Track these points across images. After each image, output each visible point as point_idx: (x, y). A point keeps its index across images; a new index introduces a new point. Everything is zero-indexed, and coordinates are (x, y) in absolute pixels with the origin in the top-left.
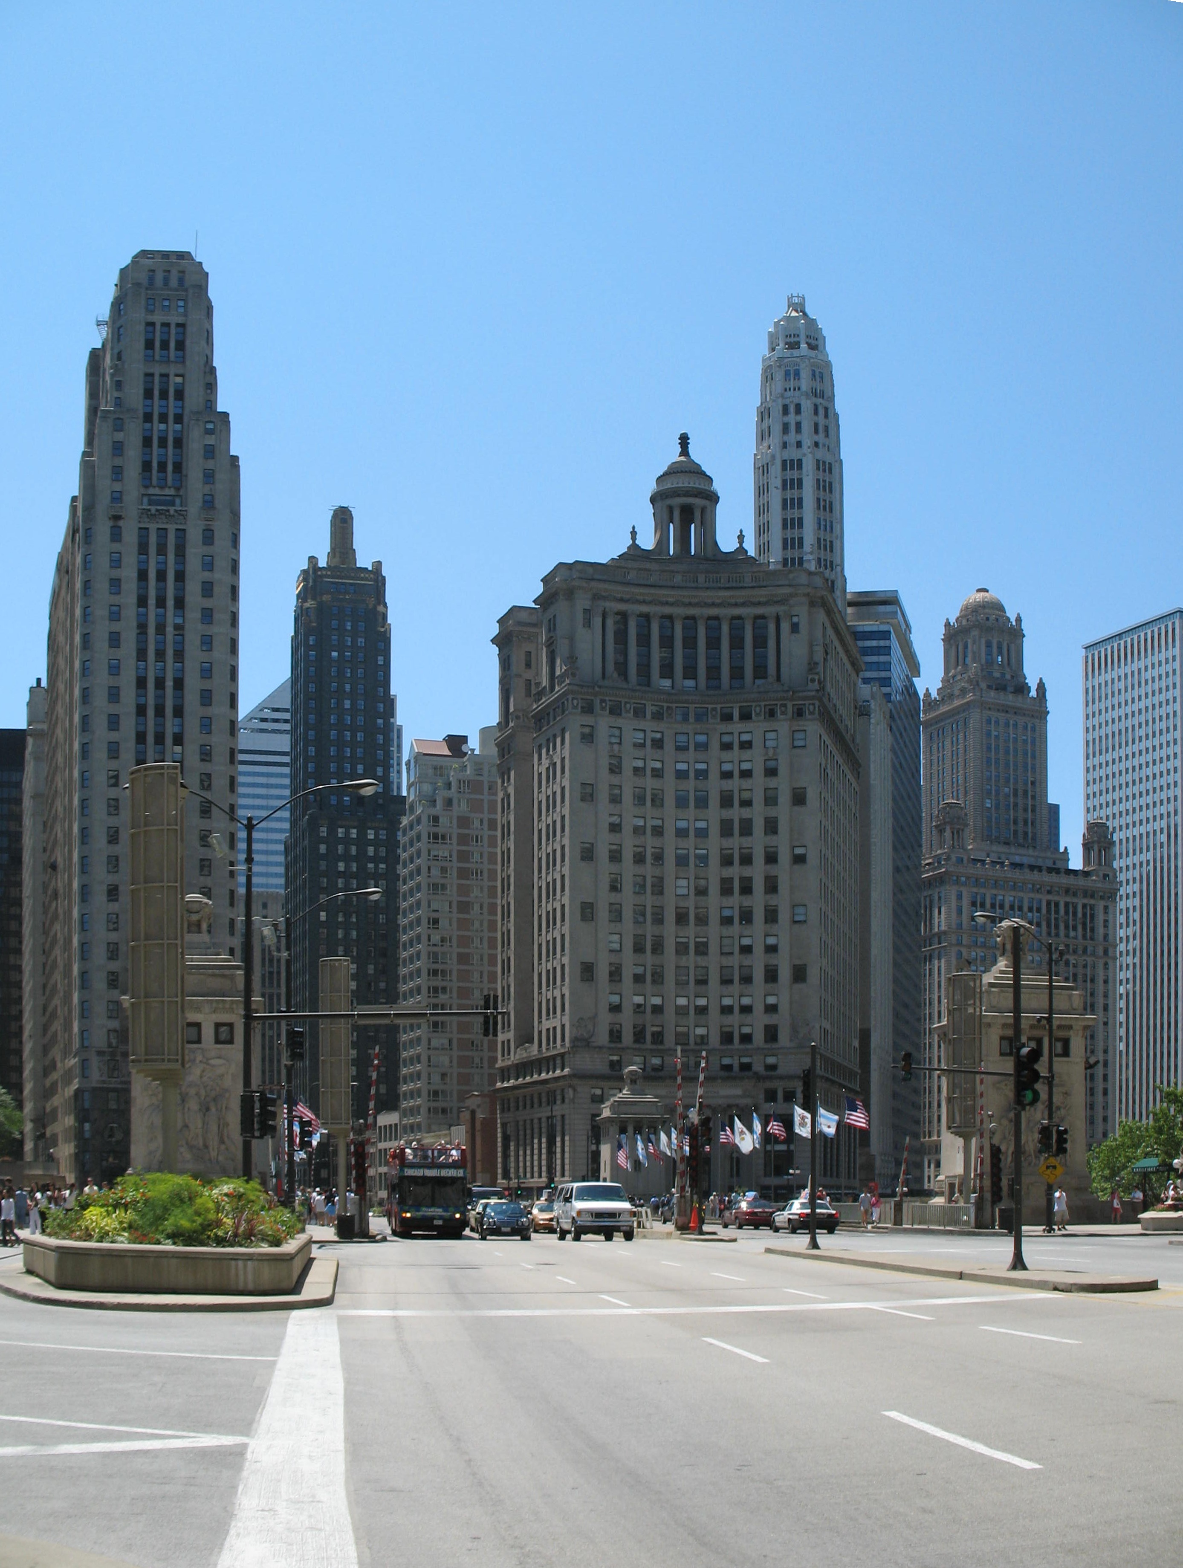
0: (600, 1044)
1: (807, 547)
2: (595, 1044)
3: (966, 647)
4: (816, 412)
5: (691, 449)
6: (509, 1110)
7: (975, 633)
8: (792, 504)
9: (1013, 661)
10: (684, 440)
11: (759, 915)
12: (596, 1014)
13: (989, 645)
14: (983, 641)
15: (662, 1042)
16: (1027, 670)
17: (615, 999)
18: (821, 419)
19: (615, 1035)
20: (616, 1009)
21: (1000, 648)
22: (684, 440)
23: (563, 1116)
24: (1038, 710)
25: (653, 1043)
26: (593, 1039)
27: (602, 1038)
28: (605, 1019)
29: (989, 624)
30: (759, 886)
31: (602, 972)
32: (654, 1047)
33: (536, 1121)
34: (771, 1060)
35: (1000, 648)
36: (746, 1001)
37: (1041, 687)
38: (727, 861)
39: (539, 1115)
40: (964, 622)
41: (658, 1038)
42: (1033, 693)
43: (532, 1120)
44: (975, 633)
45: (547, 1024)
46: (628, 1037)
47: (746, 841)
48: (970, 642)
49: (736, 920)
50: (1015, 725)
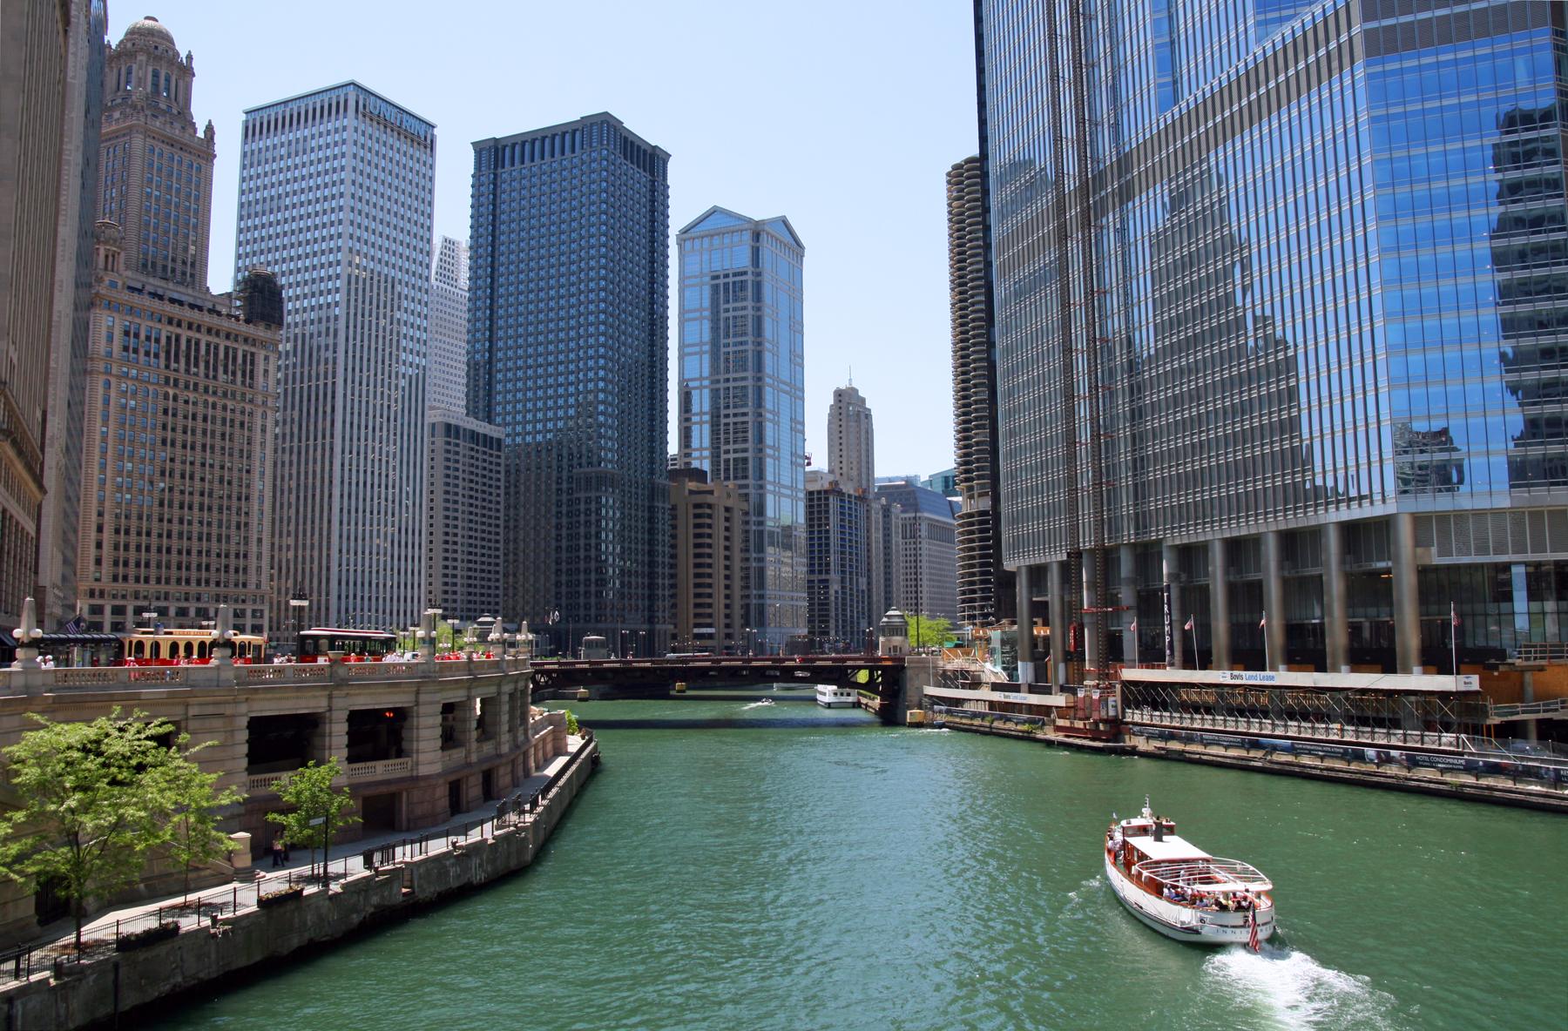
3: (129, 72)
7: (142, 58)
9: (180, 98)
13: (156, 75)
14: (150, 69)
16: (194, 109)
21: (168, 80)
24: (205, 151)
29: (158, 52)
35: (168, 80)
37: (210, 129)
40: (129, 45)
42: (200, 134)
44: (142, 58)
48: (135, 67)
50: (180, 162)
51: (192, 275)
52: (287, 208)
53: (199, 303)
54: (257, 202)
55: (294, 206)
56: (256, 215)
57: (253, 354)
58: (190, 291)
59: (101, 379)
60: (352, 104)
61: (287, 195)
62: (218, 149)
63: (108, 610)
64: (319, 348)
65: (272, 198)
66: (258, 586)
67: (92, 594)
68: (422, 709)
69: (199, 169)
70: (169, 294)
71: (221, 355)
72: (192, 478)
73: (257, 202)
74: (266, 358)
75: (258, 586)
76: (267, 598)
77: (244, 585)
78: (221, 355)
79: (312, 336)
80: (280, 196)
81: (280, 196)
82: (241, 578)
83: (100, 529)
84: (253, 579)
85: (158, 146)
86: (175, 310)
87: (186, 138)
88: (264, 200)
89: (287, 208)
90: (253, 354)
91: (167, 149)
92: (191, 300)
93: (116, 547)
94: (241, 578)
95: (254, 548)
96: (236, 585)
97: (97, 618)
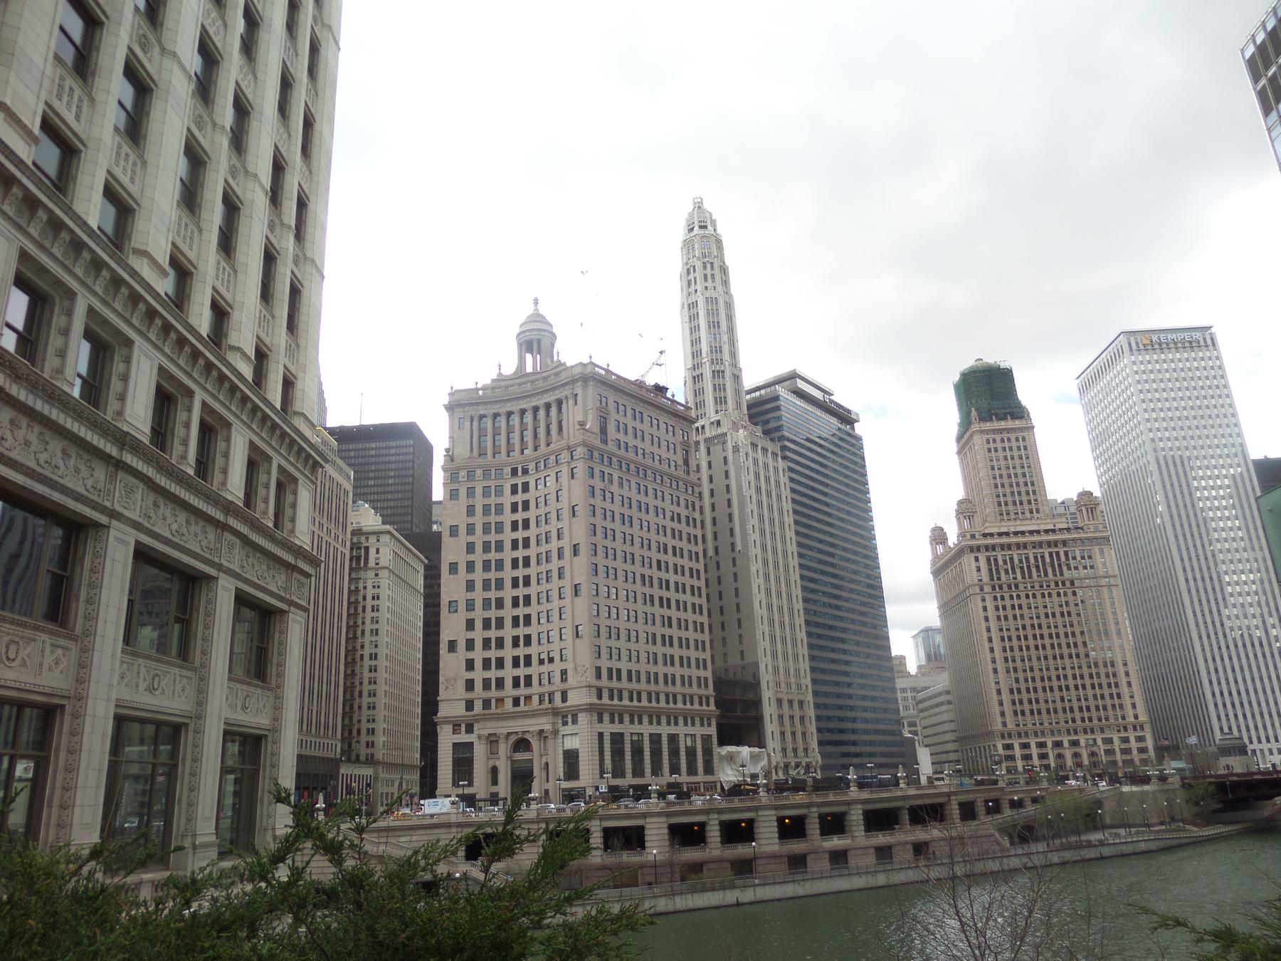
1: (704, 355)
4: (705, 268)
5: (539, 307)
8: (694, 329)
10: (536, 302)
18: (709, 271)
22: (536, 302)
59: (979, 598)
60: (1126, 347)
63: (1017, 746)
66: (1136, 717)
67: (1003, 737)
68: (648, 826)
69: (1024, 439)
70: (1012, 529)
75: (1136, 717)
77: (1123, 718)
83: (999, 692)
84: (1130, 713)
85: (991, 436)
91: (998, 437)
93: (1014, 703)
97: (1009, 752)
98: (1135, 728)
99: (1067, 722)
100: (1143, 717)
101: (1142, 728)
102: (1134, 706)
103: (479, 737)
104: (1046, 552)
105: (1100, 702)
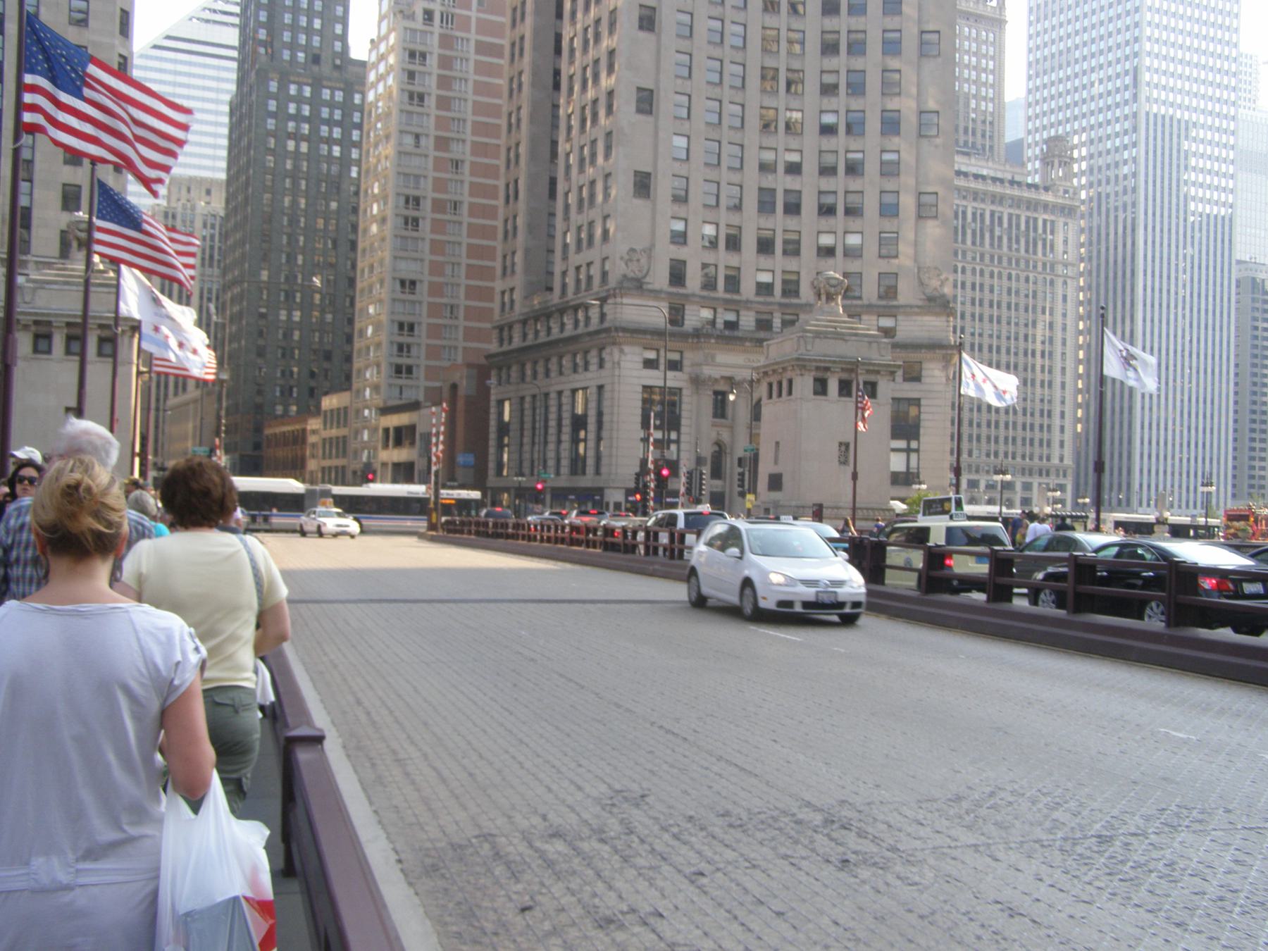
0: (657, 286)
2: (650, 287)
6: (508, 382)
11: (873, 124)
12: (652, 246)
15: (738, 291)
17: (679, 226)
19: (677, 275)
20: (680, 238)
23: (600, 388)
25: (726, 290)
26: (647, 279)
27: (660, 278)
28: (666, 252)
30: (873, 82)
31: (664, 187)
32: (728, 296)
33: (553, 396)
34: (887, 322)
36: (854, 240)
38: (830, 48)
39: (559, 388)
41: (733, 282)
43: (547, 395)
45: (575, 259)
46: (694, 281)
47: (857, 22)
49: (842, 129)
51: (991, 147)
52: (1077, 61)
53: (999, 175)
54: (1045, 59)
55: (1085, 58)
56: (1045, 73)
57: (1053, 222)
58: (990, 164)
61: (1077, 47)
62: (1009, 14)
64: (1116, 209)
65: (1061, 53)
66: (1061, 459)
71: (1023, 227)
72: (998, 351)
73: (1045, 59)
74: (1066, 224)
75: (1061, 459)
76: (1070, 472)
77: (1048, 459)
78: (1023, 227)
79: (1108, 196)
80: (1069, 50)
81: (1069, 50)
82: (1045, 451)
86: (979, 186)
87: (980, 10)
88: (1053, 56)
89: (1077, 61)
90: (1053, 222)
92: (992, 174)
94: (1045, 451)
95: (1057, 421)
96: (1041, 458)
98: (1058, 475)
99: (988, 455)
100: (1068, 461)
101: (1065, 476)
102: (1062, 444)
103: (697, 381)
104: (1006, 212)
105: (1028, 434)
